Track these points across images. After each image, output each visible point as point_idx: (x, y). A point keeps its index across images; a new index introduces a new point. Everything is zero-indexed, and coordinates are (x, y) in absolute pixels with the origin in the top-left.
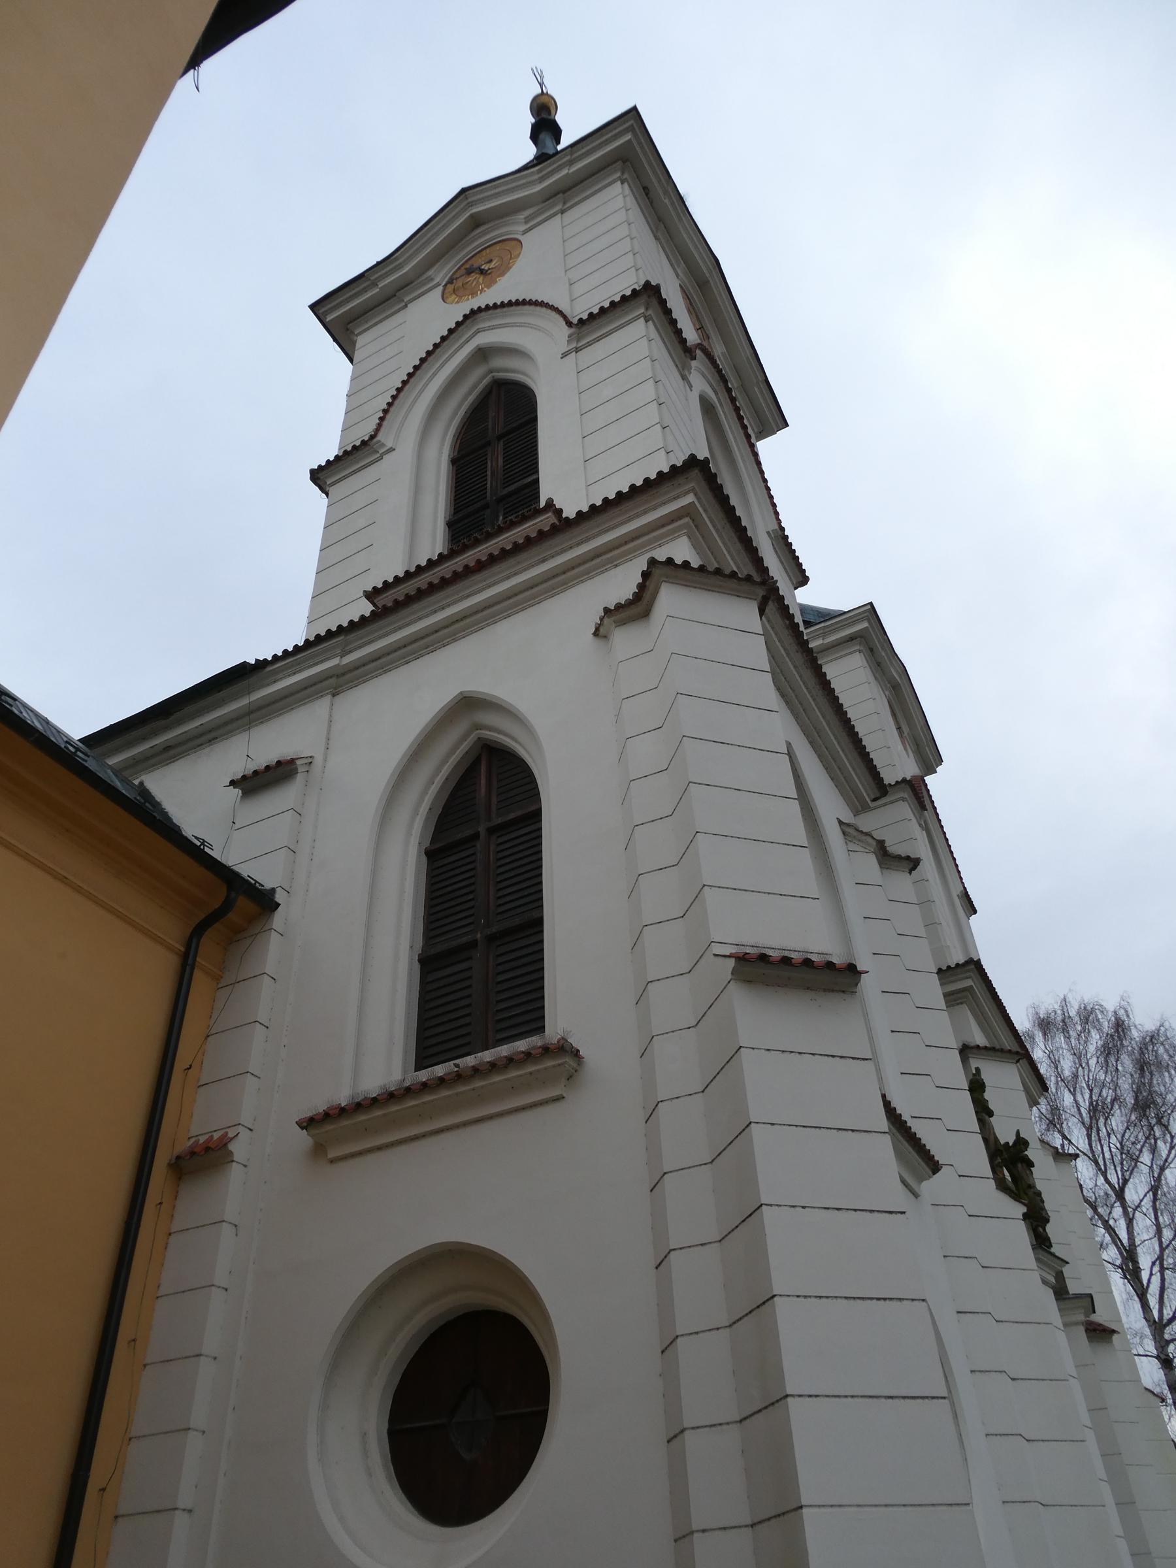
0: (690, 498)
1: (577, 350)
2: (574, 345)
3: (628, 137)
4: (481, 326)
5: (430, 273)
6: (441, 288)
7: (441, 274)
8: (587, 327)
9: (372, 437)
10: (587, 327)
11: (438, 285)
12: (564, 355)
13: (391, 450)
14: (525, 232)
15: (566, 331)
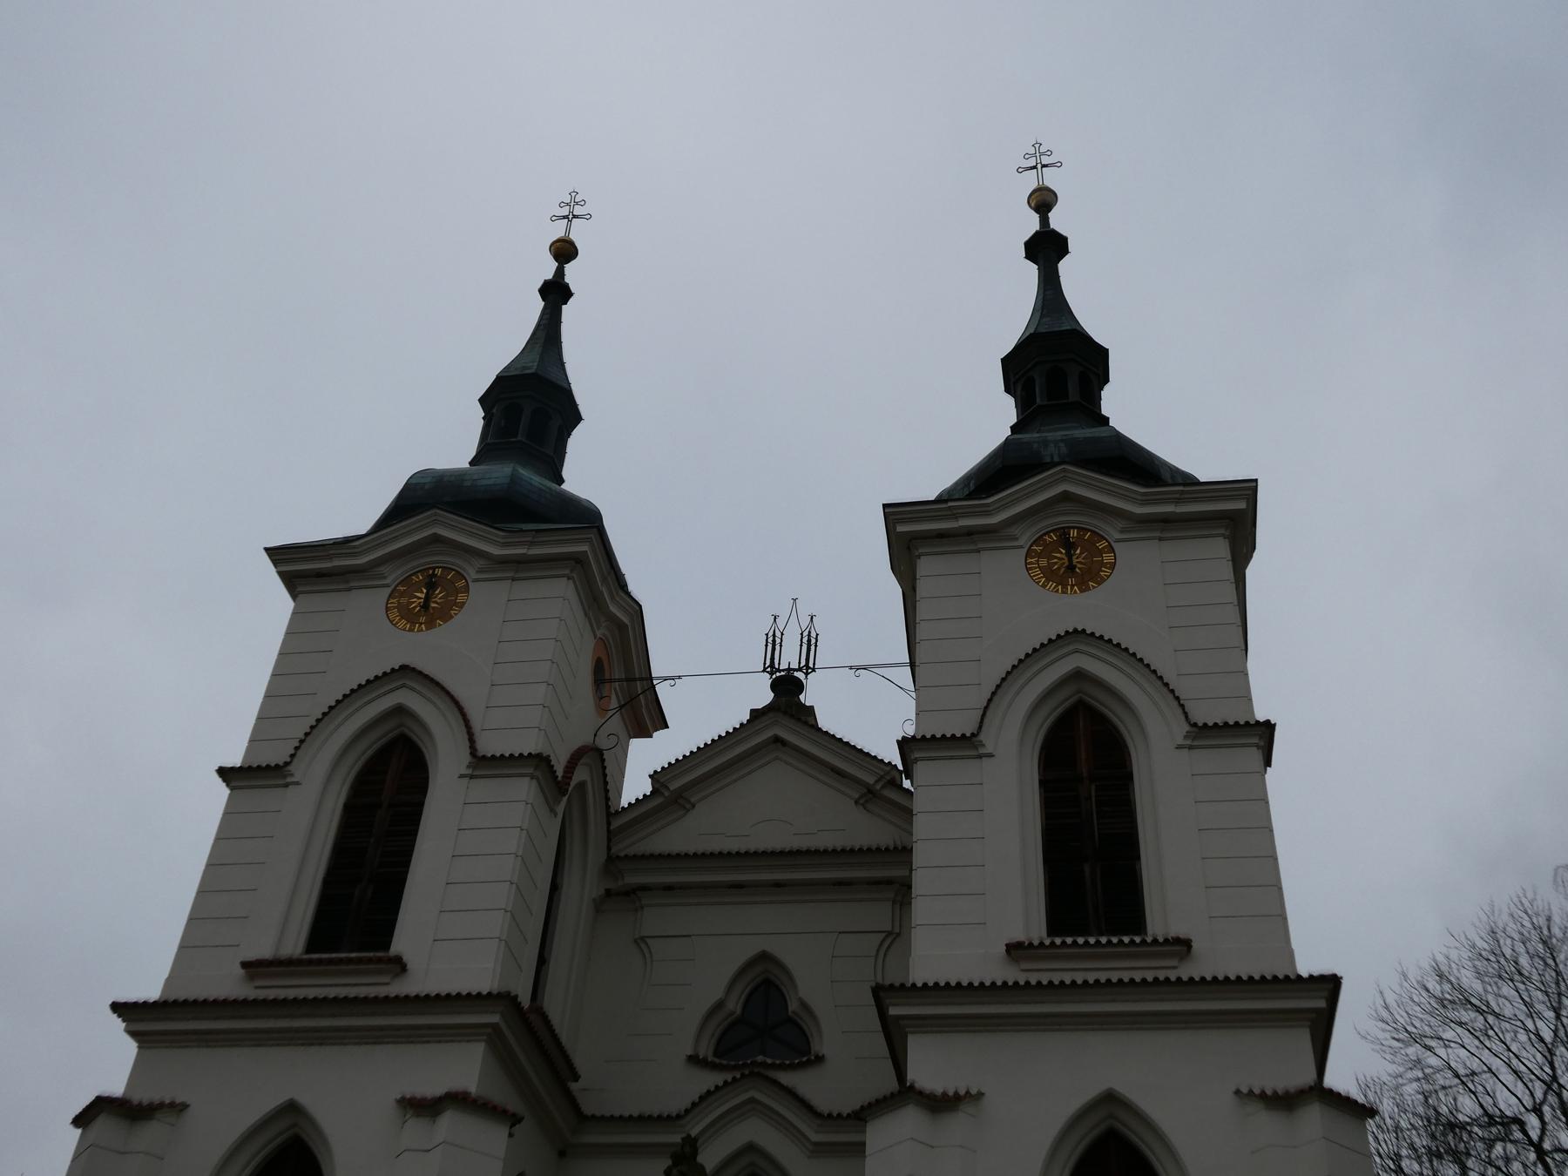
0: (495, 1019)
1: (472, 777)
2: (469, 772)
3: (585, 548)
4: (408, 683)
5: (383, 569)
6: (389, 590)
7: (394, 575)
8: (483, 764)
9: (287, 764)
10: (483, 764)
11: (387, 586)
12: (462, 776)
13: (297, 783)
14: (476, 580)
15: (466, 758)
